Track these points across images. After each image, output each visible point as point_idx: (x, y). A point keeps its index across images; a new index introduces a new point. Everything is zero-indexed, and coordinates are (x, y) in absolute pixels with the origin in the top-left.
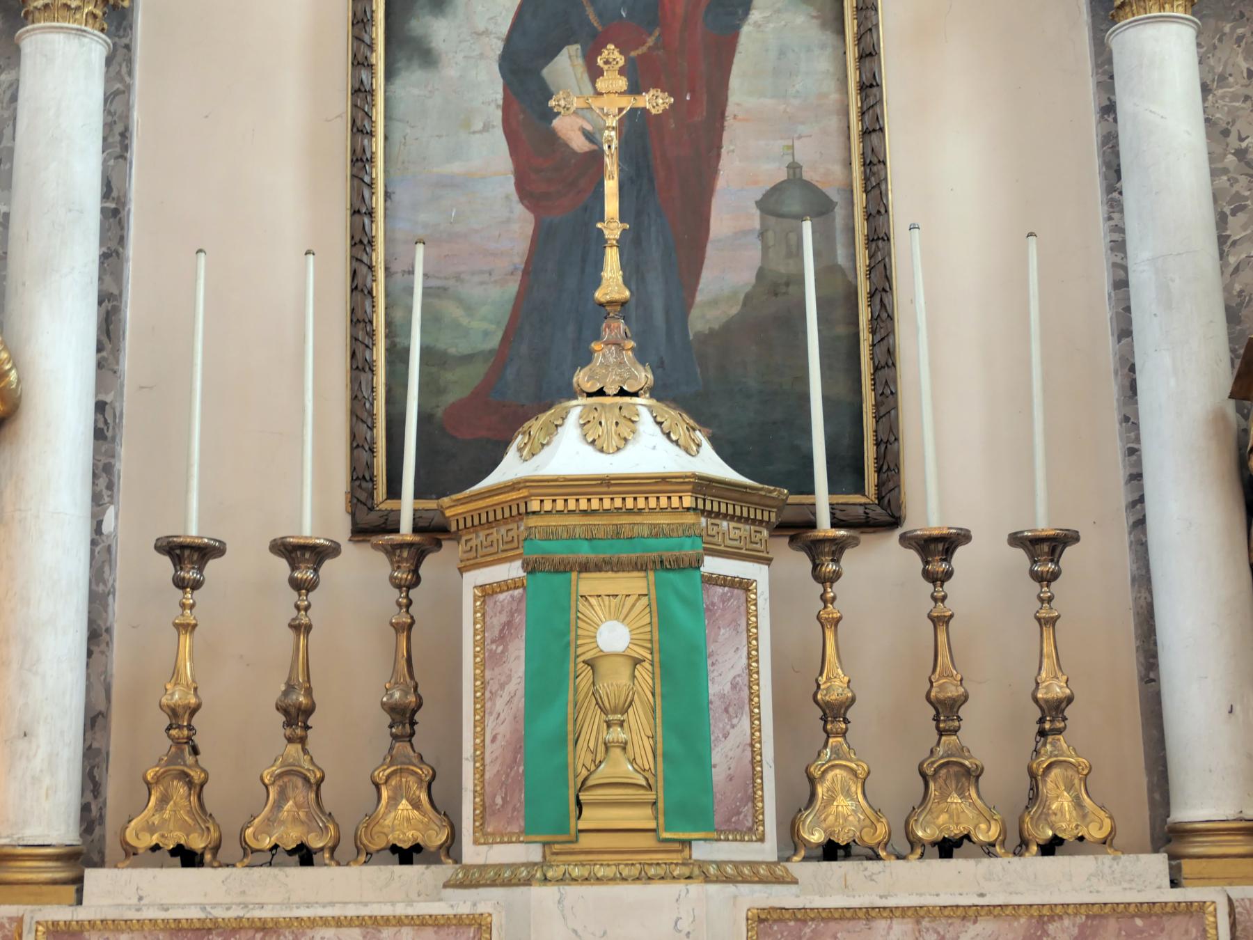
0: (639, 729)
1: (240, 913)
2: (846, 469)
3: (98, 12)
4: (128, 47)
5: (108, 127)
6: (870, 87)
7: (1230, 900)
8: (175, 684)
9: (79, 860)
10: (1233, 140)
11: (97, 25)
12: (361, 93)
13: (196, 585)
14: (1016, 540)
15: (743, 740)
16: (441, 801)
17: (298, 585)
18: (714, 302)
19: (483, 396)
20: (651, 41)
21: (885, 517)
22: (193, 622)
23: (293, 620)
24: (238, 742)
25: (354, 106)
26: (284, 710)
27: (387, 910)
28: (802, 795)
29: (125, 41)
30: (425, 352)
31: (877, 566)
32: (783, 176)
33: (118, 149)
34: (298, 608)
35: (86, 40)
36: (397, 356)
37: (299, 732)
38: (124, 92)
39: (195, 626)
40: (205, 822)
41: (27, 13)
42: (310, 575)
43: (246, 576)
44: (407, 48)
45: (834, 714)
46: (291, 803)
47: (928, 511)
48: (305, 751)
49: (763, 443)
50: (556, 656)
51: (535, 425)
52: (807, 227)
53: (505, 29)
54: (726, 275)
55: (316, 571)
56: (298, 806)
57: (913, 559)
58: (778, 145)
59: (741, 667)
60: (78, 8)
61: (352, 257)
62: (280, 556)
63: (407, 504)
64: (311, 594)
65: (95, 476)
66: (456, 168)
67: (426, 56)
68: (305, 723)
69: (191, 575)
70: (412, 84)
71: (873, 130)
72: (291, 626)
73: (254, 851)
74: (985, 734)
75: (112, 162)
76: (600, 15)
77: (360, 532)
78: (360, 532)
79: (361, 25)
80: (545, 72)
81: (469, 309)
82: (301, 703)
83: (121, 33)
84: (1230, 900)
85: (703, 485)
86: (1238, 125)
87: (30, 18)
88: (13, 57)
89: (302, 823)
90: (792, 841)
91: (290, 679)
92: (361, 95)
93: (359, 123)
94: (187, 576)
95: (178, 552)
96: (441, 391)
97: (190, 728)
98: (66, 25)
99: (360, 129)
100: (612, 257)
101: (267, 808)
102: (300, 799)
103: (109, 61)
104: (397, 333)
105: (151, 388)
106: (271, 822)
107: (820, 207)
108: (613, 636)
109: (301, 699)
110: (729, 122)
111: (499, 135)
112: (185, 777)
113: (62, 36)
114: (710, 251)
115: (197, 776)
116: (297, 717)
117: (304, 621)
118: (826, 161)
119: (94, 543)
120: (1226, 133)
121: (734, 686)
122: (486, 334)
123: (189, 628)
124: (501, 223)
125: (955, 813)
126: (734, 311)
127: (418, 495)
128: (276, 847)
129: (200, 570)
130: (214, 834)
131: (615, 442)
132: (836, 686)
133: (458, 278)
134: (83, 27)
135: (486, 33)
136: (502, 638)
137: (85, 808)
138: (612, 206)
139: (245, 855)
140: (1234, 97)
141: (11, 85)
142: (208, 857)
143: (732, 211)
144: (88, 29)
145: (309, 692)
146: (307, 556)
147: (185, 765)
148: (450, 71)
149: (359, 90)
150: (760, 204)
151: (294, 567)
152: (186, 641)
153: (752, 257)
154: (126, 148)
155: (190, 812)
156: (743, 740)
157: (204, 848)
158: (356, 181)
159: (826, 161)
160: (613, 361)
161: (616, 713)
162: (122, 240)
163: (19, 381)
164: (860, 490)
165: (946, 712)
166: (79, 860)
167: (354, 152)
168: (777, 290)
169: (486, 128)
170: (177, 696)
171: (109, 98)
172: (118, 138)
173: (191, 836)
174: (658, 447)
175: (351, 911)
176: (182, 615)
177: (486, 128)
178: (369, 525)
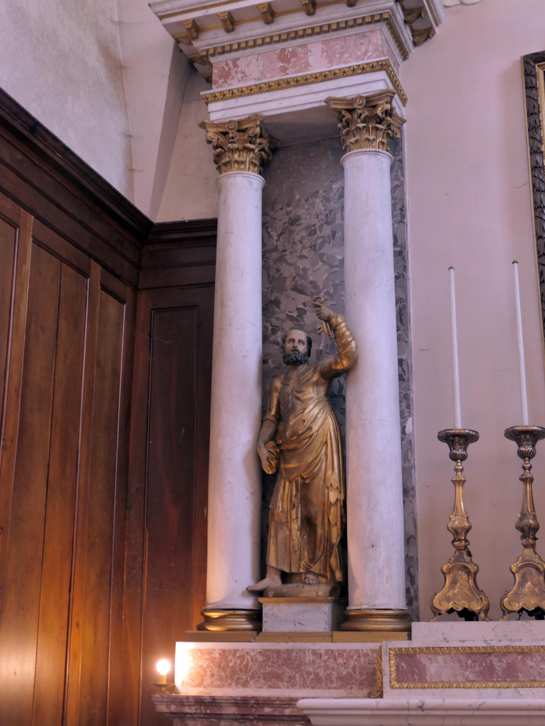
1: (508, 644)
3: (385, 141)
4: (401, 161)
5: (394, 205)
8: (456, 515)
9: (406, 619)
11: (385, 148)
13: (463, 458)
17: (523, 455)
22: (463, 479)
23: (522, 475)
25: (534, 176)
26: (521, 529)
29: (399, 157)
33: (399, 218)
34: (524, 468)
35: (379, 157)
37: (531, 541)
38: (400, 186)
39: (464, 481)
40: (479, 595)
41: (346, 147)
42: (530, 449)
46: (529, 583)
48: (536, 553)
55: (533, 446)
56: (535, 585)
60: (374, 140)
61: (539, 264)
62: (511, 439)
64: (531, 460)
65: (401, 402)
68: (534, 536)
69: (460, 452)
72: (521, 479)
73: (510, 612)
75: (396, 225)
79: (534, 130)
82: (531, 524)
83: (396, 153)
87: (348, 149)
88: (339, 171)
89: (537, 595)
91: (523, 510)
92: (537, 170)
93: (537, 186)
94: (458, 453)
95: (451, 438)
97: (466, 540)
98: (368, 149)
101: (515, 587)
102: (535, 580)
103: (392, 168)
105: (427, 350)
106: (517, 596)
109: (531, 521)
112: (465, 569)
113: (366, 156)
115: (472, 568)
116: (529, 532)
117: (529, 475)
119: (402, 439)
123: (462, 483)
128: (522, 609)
129: (465, 449)
130: (485, 602)
134: (377, 150)
137: (408, 591)
139: (504, 614)
141: (339, 190)
142: (482, 615)
144: (380, 150)
145: (535, 518)
146: (528, 437)
147: (465, 562)
149: (536, 167)
151: (520, 445)
152: (460, 490)
154: (403, 216)
155: (470, 589)
157: (480, 610)
158: (538, 220)
162: (405, 268)
163: (357, 347)
166: (406, 619)
167: (535, 203)
170: (456, 523)
171: (394, 189)
172: (399, 212)
173: (472, 603)
176: (457, 475)
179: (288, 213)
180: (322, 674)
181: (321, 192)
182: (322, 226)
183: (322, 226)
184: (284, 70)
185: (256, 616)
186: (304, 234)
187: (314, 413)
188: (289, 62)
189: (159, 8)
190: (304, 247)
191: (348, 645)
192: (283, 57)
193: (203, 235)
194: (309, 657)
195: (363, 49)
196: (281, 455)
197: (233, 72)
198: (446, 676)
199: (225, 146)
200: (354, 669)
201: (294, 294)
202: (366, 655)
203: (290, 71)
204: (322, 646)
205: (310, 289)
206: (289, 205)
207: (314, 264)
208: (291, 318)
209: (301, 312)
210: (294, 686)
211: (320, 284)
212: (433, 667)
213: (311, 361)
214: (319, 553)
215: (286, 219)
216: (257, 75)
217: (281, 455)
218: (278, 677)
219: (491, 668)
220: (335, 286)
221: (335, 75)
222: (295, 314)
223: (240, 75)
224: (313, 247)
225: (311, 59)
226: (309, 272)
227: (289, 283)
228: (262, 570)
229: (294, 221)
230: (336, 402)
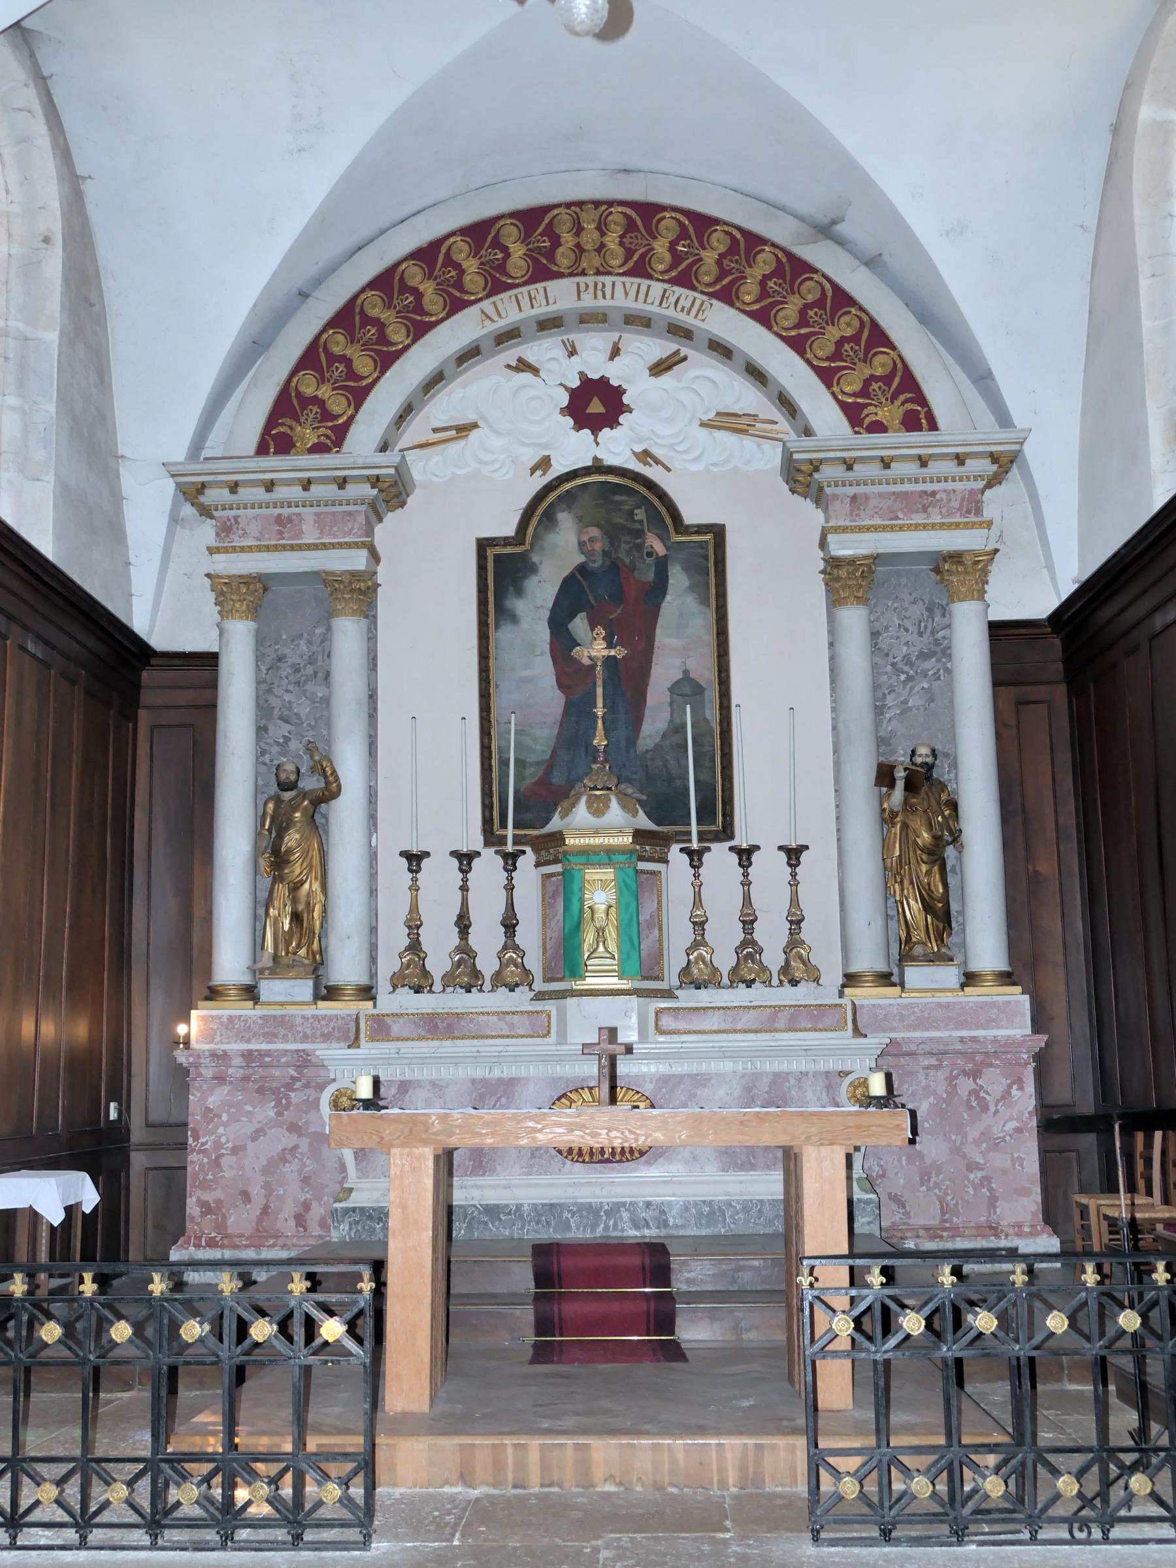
2: (706, 812)
7: (853, 1003)
10: (890, 658)
14: (780, 848)
18: (649, 736)
19: (544, 781)
20: (619, 611)
21: (727, 833)
27: (508, 1009)
30: (516, 760)
32: (680, 676)
36: (505, 763)
44: (506, 615)
51: (566, 803)
52: (688, 707)
53: (550, 605)
54: (654, 726)
57: (734, 858)
58: (678, 662)
63: (510, 832)
66: (529, 673)
67: (514, 618)
76: (595, 598)
77: (487, 843)
78: (487, 843)
80: (570, 626)
81: (535, 740)
84: (853, 1003)
86: (894, 651)
96: (524, 779)
97: (418, 934)
100: (600, 723)
104: (504, 751)
107: (698, 690)
110: (656, 650)
111: (548, 655)
114: (647, 712)
120: (887, 655)
121: (651, 916)
122: (544, 751)
126: (658, 740)
127: (515, 827)
133: (530, 725)
135: (542, 607)
136: (554, 895)
138: (600, 703)
140: (892, 637)
148: (525, 624)
150: (671, 690)
153: (666, 715)
154: (375, 665)
162: (375, 709)
164: (714, 822)
168: (679, 729)
169: (542, 654)
175: (493, 1010)
177: (542, 654)
178: (491, 837)
179: (276, 651)
180: (309, 1032)
181: (305, 635)
182: (305, 666)
183: (305, 666)
184: (280, 533)
186: (289, 671)
188: (285, 527)
189: (171, 468)
190: (290, 683)
194: (299, 1021)
195: (350, 525)
197: (234, 529)
198: (405, 1034)
200: (333, 1029)
201: (281, 723)
202: (343, 1018)
203: (286, 535)
204: (310, 1011)
205: (294, 720)
206: (276, 643)
207: (299, 698)
208: (278, 743)
209: (287, 739)
210: (287, 1041)
211: (303, 717)
212: (395, 1029)
214: (304, 941)
215: (274, 656)
216: (257, 534)
218: (275, 1035)
219: (436, 1026)
220: (316, 719)
221: (324, 546)
222: (281, 741)
223: (240, 532)
224: (298, 683)
225: (304, 527)
226: (294, 705)
227: (276, 713)
229: (281, 659)
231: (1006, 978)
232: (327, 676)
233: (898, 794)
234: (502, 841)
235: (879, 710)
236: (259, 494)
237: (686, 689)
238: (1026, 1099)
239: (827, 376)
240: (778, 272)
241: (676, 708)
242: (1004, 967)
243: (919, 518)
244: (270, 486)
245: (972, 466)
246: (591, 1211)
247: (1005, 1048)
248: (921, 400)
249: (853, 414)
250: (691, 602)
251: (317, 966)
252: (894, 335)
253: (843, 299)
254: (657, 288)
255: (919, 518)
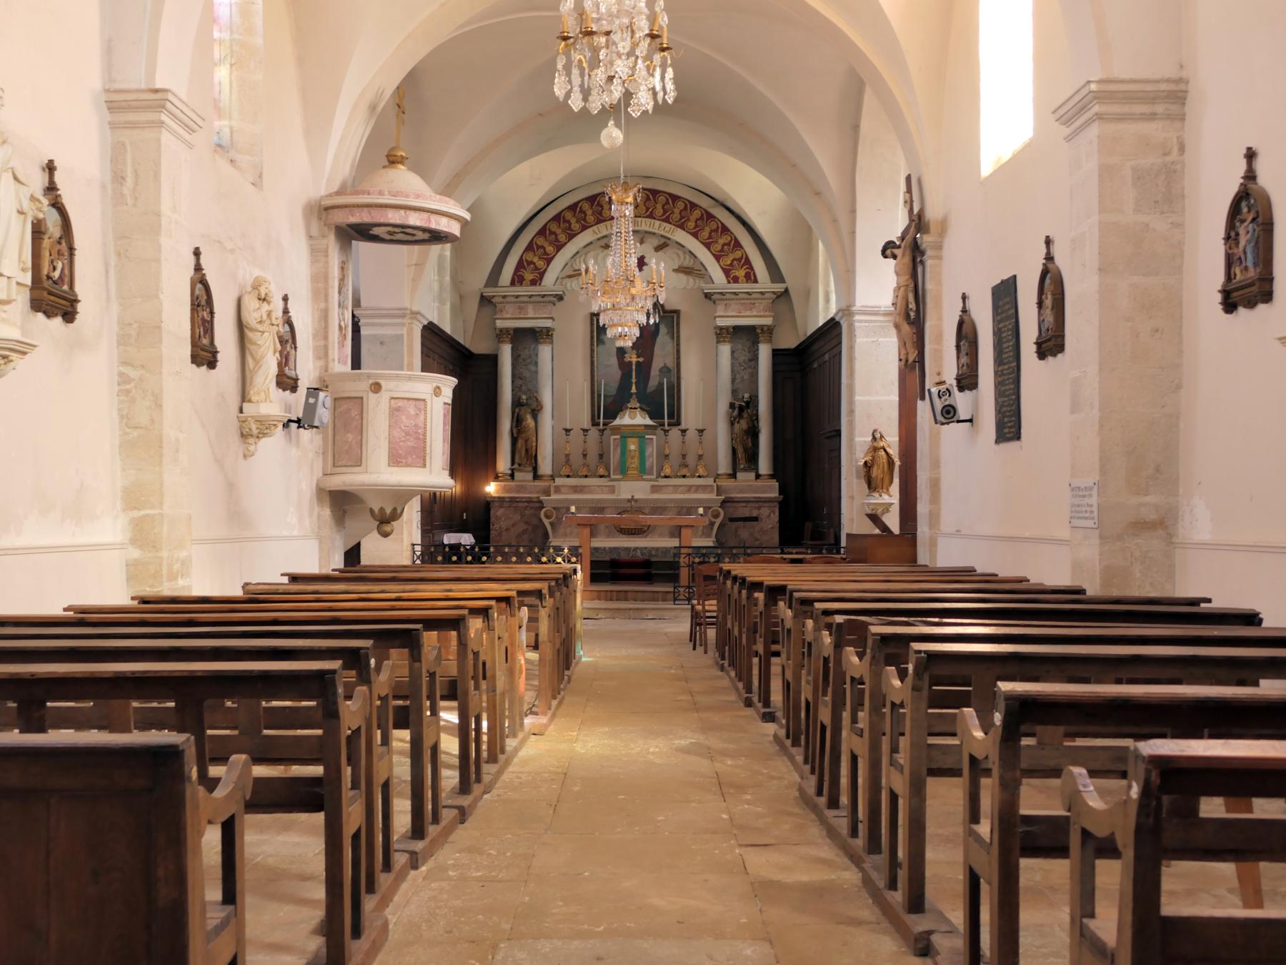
0: (636, 461)
2: (671, 416)
6: (678, 351)
9: (552, 477)
12: (592, 351)
15: (652, 461)
16: (608, 469)
21: (678, 423)
24: (576, 459)
28: (661, 469)
31: (675, 432)
36: (599, 396)
43: (576, 435)
45: (667, 456)
47: (683, 426)
49: (655, 414)
50: (624, 450)
54: (653, 383)
59: (652, 451)
67: (603, 343)
70: (601, 347)
71: (678, 358)
74: (691, 460)
85: (647, 426)
90: (659, 476)
99: (592, 357)
104: (599, 391)
107: (669, 370)
108: (632, 447)
116: (585, 456)
118: (671, 363)
124: (616, 373)
125: (684, 471)
131: (634, 418)
132: (667, 452)
143: (655, 372)
156: (652, 461)
159: (671, 363)
160: (634, 403)
161: (633, 458)
165: (684, 456)
166: (552, 477)
168: (661, 384)
174: (641, 419)
178: (595, 424)
185: (512, 476)
187: (529, 421)
191: (538, 483)
192: (520, 308)
193: (493, 360)
196: (519, 432)
199: (501, 335)
213: (527, 406)
217: (519, 432)
228: (513, 463)
230: (535, 418)
231: (772, 476)
232: (536, 364)
233: (736, 412)
234: (598, 424)
235: (733, 380)
236: (513, 299)
237: (665, 370)
238: (775, 517)
239: (718, 258)
240: (701, 218)
241: (661, 378)
242: (771, 472)
243: (748, 313)
244: (517, 297)
245: (767, 295)
246: (628, 549)
247: (770, 500)
248: (751, 268)
249: (727, 272)
250: (667, 338)
251: (535, 469)
252: (743, 243)
253: (725, 229)
254: (657, 223)
255: (748, 313)
